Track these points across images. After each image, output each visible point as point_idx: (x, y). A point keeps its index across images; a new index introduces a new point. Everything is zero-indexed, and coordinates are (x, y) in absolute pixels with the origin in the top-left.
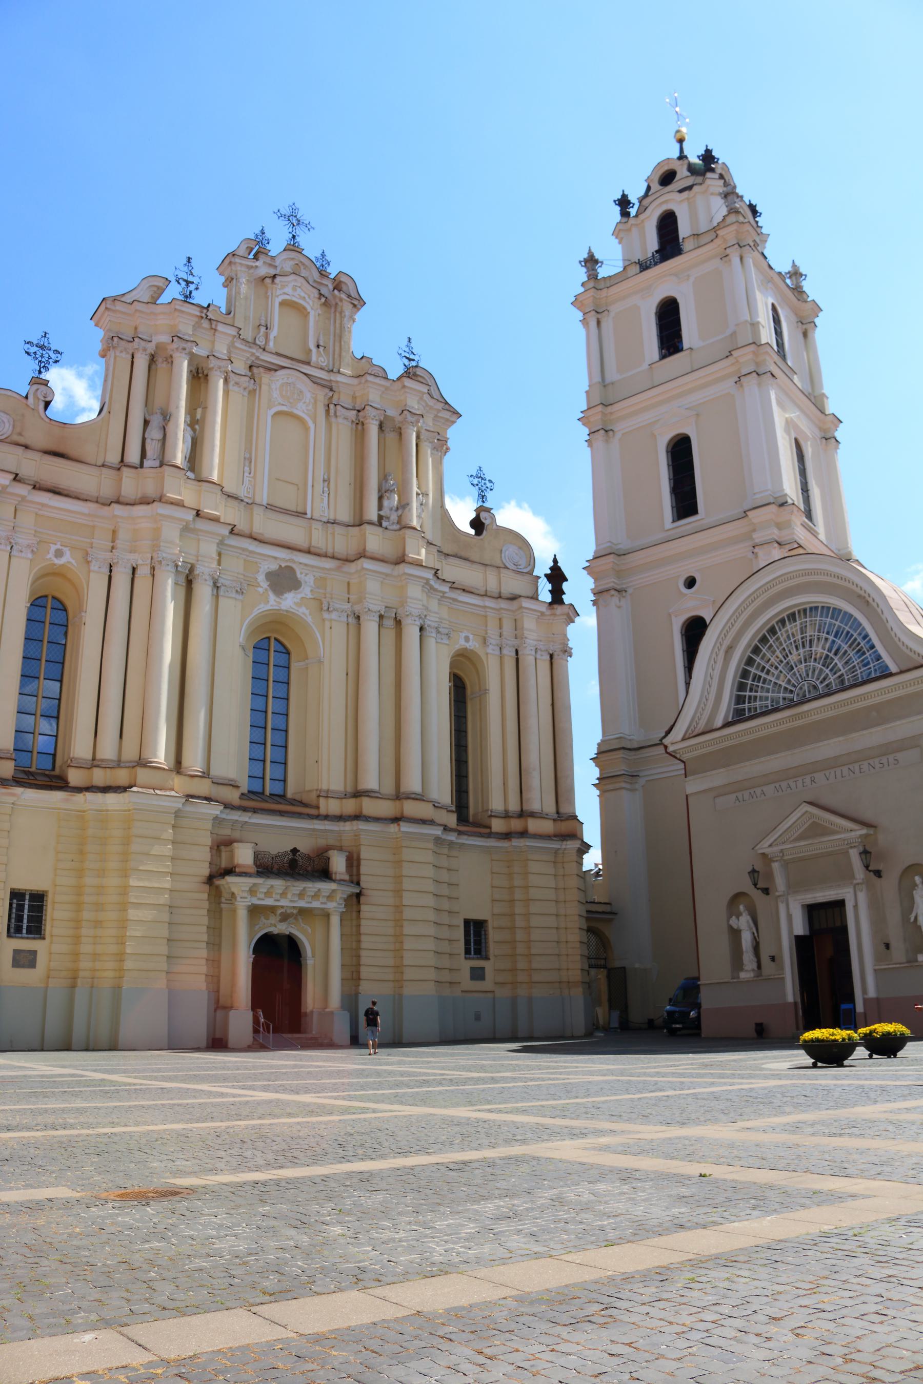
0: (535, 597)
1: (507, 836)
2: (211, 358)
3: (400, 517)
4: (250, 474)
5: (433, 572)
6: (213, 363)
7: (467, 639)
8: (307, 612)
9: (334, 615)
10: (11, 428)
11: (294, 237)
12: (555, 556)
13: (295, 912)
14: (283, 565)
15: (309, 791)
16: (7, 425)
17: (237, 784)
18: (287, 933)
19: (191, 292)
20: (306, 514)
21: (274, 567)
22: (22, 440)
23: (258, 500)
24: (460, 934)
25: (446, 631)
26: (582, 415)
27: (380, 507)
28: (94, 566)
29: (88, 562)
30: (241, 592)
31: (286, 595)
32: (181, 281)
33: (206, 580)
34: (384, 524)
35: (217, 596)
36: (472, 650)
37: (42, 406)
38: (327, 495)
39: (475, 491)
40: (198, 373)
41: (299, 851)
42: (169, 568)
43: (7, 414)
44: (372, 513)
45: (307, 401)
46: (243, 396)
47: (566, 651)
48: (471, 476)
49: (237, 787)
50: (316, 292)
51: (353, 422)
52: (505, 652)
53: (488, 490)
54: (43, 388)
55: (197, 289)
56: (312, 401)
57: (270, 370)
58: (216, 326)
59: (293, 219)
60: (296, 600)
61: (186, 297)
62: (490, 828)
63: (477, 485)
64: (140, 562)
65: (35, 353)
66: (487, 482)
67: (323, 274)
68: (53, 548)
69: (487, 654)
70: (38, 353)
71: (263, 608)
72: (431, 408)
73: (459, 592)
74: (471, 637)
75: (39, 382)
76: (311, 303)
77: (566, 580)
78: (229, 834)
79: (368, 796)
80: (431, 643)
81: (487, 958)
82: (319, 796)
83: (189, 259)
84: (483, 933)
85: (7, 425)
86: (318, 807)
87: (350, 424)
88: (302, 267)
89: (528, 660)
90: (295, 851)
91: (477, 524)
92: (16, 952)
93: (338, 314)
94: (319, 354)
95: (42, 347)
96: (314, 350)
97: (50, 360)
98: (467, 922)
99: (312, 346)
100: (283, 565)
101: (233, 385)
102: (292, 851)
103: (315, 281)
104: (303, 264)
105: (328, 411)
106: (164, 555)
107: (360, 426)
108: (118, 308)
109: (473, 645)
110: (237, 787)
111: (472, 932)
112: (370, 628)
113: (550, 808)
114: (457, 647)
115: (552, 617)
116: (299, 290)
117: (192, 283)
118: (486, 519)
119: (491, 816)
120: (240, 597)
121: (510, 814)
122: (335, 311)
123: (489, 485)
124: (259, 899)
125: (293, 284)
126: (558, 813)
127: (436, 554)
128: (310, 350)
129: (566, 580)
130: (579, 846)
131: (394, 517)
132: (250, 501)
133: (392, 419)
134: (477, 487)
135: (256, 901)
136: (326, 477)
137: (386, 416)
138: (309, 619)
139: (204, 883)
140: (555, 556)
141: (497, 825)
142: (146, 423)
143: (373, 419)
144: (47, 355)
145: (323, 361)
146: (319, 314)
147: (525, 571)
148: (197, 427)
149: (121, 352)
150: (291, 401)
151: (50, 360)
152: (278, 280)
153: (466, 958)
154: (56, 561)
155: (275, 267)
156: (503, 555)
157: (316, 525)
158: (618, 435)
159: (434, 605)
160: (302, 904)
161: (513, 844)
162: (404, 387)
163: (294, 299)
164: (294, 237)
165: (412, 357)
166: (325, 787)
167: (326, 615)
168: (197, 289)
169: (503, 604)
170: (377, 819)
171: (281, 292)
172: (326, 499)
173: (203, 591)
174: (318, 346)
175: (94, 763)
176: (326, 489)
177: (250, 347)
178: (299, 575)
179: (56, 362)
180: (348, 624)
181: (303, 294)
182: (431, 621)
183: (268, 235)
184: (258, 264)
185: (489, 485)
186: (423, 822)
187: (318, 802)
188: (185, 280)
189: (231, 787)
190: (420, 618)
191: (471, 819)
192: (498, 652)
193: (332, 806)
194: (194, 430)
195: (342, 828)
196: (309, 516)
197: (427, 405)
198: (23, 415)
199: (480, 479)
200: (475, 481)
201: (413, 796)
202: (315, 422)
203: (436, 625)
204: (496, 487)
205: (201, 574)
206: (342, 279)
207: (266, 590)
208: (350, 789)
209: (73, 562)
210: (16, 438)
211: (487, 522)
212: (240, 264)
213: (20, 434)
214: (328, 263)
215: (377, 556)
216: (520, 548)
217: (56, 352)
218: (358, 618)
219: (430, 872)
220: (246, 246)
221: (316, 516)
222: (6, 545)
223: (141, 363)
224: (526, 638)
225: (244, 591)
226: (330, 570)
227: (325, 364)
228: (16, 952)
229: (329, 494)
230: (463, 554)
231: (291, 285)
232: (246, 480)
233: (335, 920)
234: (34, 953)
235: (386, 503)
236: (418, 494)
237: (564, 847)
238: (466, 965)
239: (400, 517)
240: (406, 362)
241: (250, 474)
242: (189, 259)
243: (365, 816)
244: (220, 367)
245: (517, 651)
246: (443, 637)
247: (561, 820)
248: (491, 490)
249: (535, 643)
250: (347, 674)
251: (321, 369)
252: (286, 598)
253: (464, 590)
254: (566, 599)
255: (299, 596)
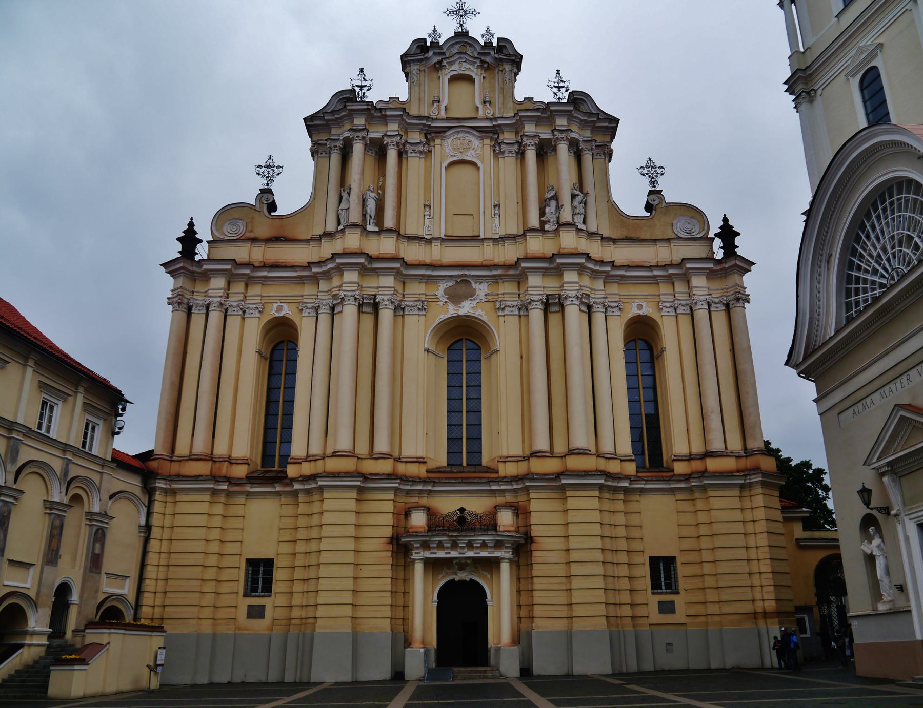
0: (710, 258)
1: (687, 478)
2: (385, 138)
3: (558, 218)
4: (430, 216)
5: (585, 256)
6: (386, 140)
7: (640, 307)
8: (483, 313)
9: (506, 312)
10: (245, 229)
11: (461, 25)
12: (725, 215)
13: (468, 561)
14: (459, 281)
15: (495, 458)
16: (242, 228)
17: (425, 460)
18: (468, 579)
19: (364, 93)
20: (479, 236)
21: (451, 283)
22: (252, 235)
23: (436, 235)
24: (646, 570)
25: (617, 304)
26: (786, 87)
27: (542, 213)
28: (305, 313)
29: (302, 310)
30: (422, 309)
31: (463, 303)
32: (356, 88)
33: (386, 305)
34: (547, 227)
35: (403, 316)
36: (646, 316)
37: (265, 207)
38: (498, 217)
39: (646, 181)
40: (382, 152)
41: (465, 510)
42: (349, 302)
43: (241, 220)
44: (534, 222)
45: (476, 147)
46: (420, 158)
47: (738, 299)
48: (640, 168)
49: (425, 462)
50: (478, 63)
51: (517, 153)
52: (678, 312)
53: (659, 175)
54: (270, 195)
55: (368, 90)
56: (481, 146)
57: (440, 132)
58: (385, 111)
59: (461, 12)
60: (472, 306)
61: (361, 98)
62: (673, 471)
63: (647, 174)
64: (335, 302)
65: (263, 172)
66: (657, 169)
67: (488, 45)
68: (275, 305)
69: (662, 316)
70: (266, 172)
71: (443, 317)
72: (586, 121)
73: (625, 268)
74: (644, 305)
75: (266, 192)
76: (475, 70)
77: (739, 234)
78: (417, 501)
79: (536, 457)
80: (599, 318)
81: (678, 593)
82: (498, 461)
83: (362, 70)
84: (672, 568)
85: (242, 228)
86: (498, 472)
87: (515, 155)
88: (468, 46)
89: (701, 314)
90: (462, 510)
91: (649, 207)
92: (250, 606)
93: (500, 72)
94: (485, 108)
95: (268, 167)
96: (480, 107)
97: (275, 174)
98: (655, 562)
99: (478, 103)
100: (459, 281)
101: (411, 153)
102: (458, 510)
103: (479, 53)
104: (468, 43)
105: (494, 151)
106: (345, 293)
107: (521, 154)
108: (315, 123)
109: (647, 310)
110: (425, 462)
111: (662, 568)
112: (536, 315)
113: (735, 444)
114: (630, 315)
115: (724, 272)
116: (464, 64)
117: (365, 86)
118: (654, 201)
119: (674, 460)
120: (423, 313)
121: (692, 457)
122: (499, 70)
123: (659, 171)
124: (432, 553)
125: (459, 61)
126: (745, 449)
127: (600, 241)
128: (478, 107)
129: (739, 234)
130: (761, 479)
131: (553, 219)
132: (428, 237)
133: (549, 141)
134: (647, 176)
135: (428, 555)
136: (497, 203)
137: (541, 140)
138: (485, 318)
139: (388, 543)
140: (725, 215)
141: (680, 468)
142: (341, 198)
143: (529, 145)
144: (272, 171)
145: (489, 112)
146: (484, 78)
147: (699, 236)
148: (380, 191)
149: (322, 153)
150: (461, 150)
151: (275, 174)
152: (445, 63)
153: (653, 593)
154: (277, 315)
155: (444, 54)
156: (674, 227)
157: (486, 243)
158: (819, 92)
159: (599, 285)
160: (470, 554)
161: (693, 484)
162: (552, 111)
163: (461, 72)
164: (461, 25)
165: (561, 84)
166: (505, 453)
167: (500, 313)
168: (368, 90)
169: (671, 271)
170: (543, 477)
171: (449, 71)
172: (497, 220)
173: (386, 315)
174: (484, 102)
175: (308, 458)
176: (497, 212)
177: (420, 120)
178: (474, 285)
179: (279, 174)
180: (520, 316)
181: (468, 66)
182: (596, 298)
183: (439, 31)
184: (426, 55)
185: (659, 171)
186: (586, 474)
187: (498, 465)
188: (357, 86)
189: (418, 464)
190: (578, 298)
191: (665, 465)
192: (674, 314)
193: (509, 469)
194: (378, 194)
195: (515, 487)
196: (482, 237)
197: (582, 121)
198: (253, 218)
199: (650, 169)
200: (645, 171)
201: (576, 451)
202: (483, 162)
203: (602, 300)
204: (666, 171)
205: (381, 301)
206: (500, 44)
207: (446, 302)
208: (527, 453)
209: (290, 313)
210: (249, 235)
211: (655, 203)
212: (411, 60)
213: (251, 231)
214: (493, 35)
215: (537, 255)
216: (692, 217)
217: (280, 167)
218: (527, 309)
219: (596, 517)
220: (417, 45)
221: (488, 235)
222: (238, 311)
223: (335, 157)
224: (694, 295)
225: (425, 307)
226: (500, 276)
227: (491, 114)
228: (250, 606)
229: (499, 215)
230: (633, 235)
231: (457, 63)
232: (427, 221)
233: (505, 567)
234: (263, 607)
235: (547, 210)
236: (573, 196)
237: (748, 481)
238: (654, 600)
239: (558, 218)
240: (556, 90)
241: (430, 216)
242: (362, 70)
243: (533, 474)
244: (392, 142)
245: (691, 308)
246: (614, 310)
247: (746, 457)
248: (662, 174)
249: (706, 297)
250: (521, 357)
251: (487, 119)
252: (463, 307)
253: (628, 266)
254: (739, 251)
255: (475, 302)
